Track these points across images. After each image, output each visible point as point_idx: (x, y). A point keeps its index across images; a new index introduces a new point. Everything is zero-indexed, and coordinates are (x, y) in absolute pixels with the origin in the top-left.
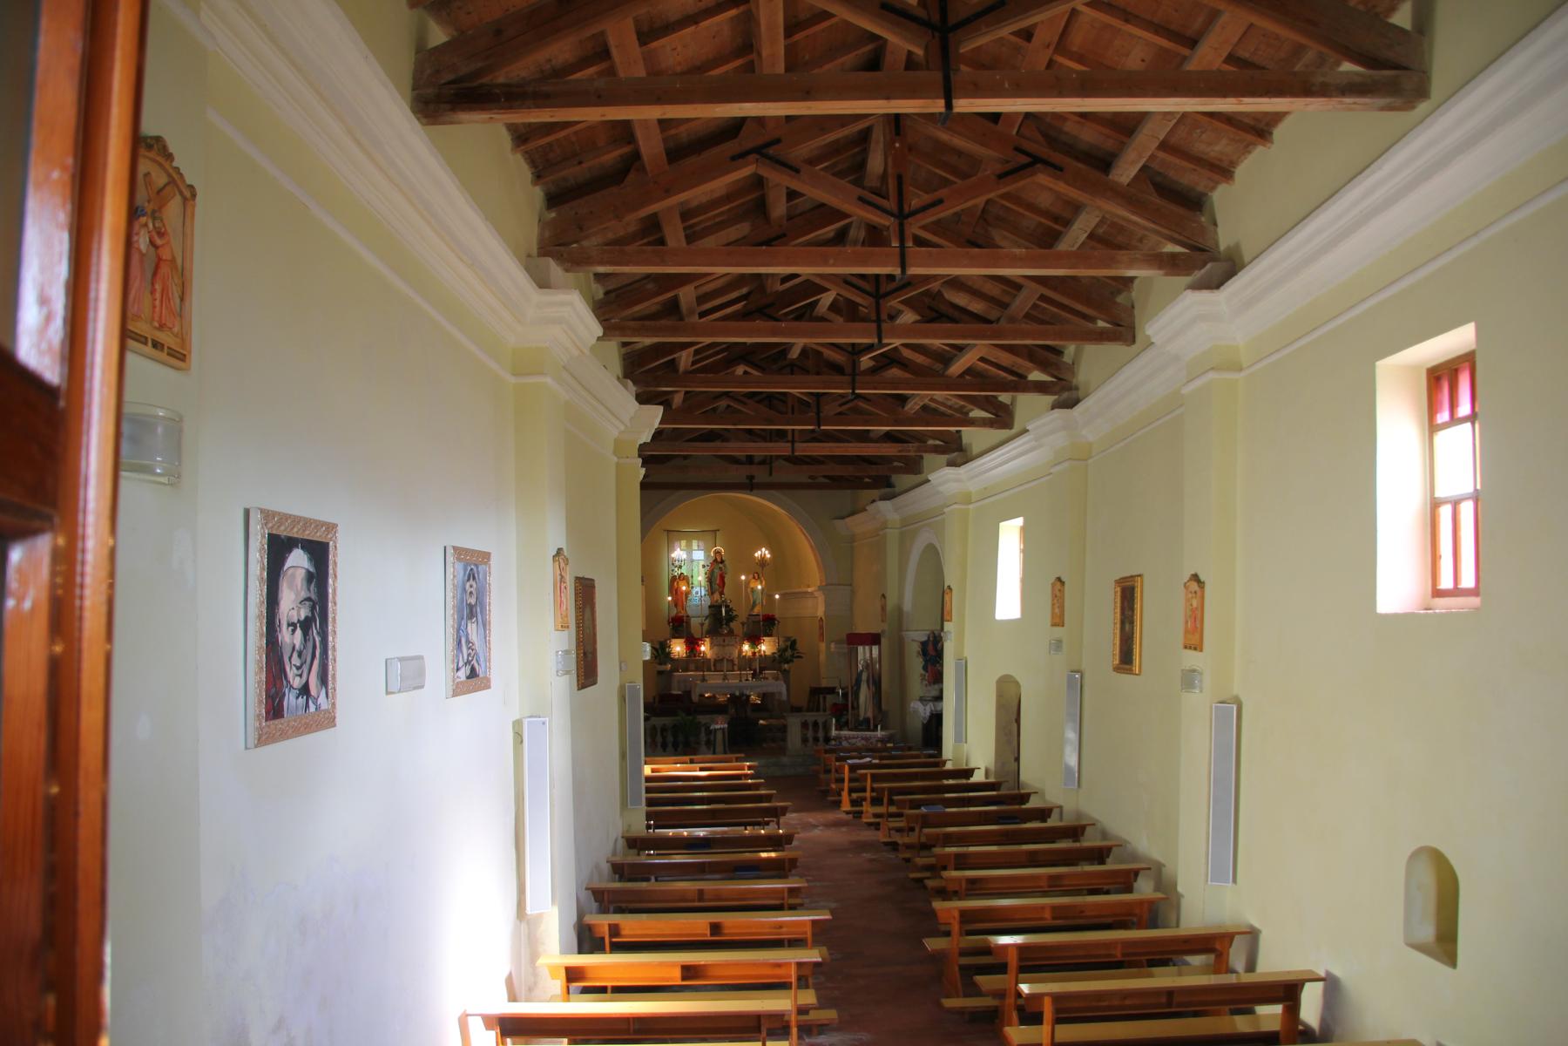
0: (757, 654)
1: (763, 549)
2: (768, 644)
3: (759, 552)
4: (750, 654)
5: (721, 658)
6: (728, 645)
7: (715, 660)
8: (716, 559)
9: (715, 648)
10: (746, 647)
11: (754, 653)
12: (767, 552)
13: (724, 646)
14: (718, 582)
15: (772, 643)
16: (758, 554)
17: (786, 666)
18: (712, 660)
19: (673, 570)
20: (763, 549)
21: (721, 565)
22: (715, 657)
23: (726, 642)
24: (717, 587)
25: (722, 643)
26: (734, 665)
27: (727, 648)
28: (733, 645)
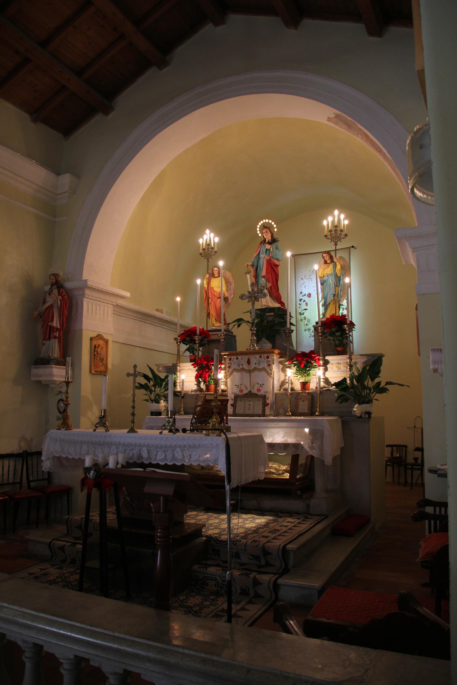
0: (313, 386)
1: (336, 212)
2: (335, 369)
3: (330, 219)
4: (298, 387)
5: (245, 392)
6: (255, 369)
7: (236, 397)
8: (265, 240)
9: (237, 375)
10: (291, 372)
11: (304, 385)
12: (342, 216)
13: (250, 372)
14: (264, 273)
15: (341, 366)
16: (328, 222)
17: (357, 409)
18: (230, 396)
19: (300, 300)
20: (336, 212)
21: (268, 247)
22: (237, 391)
23: (253, 366)
24: (263, 281)
25: (246, 366)
26: (265, 405)
27: (253, 374)
28: (264, 369)
